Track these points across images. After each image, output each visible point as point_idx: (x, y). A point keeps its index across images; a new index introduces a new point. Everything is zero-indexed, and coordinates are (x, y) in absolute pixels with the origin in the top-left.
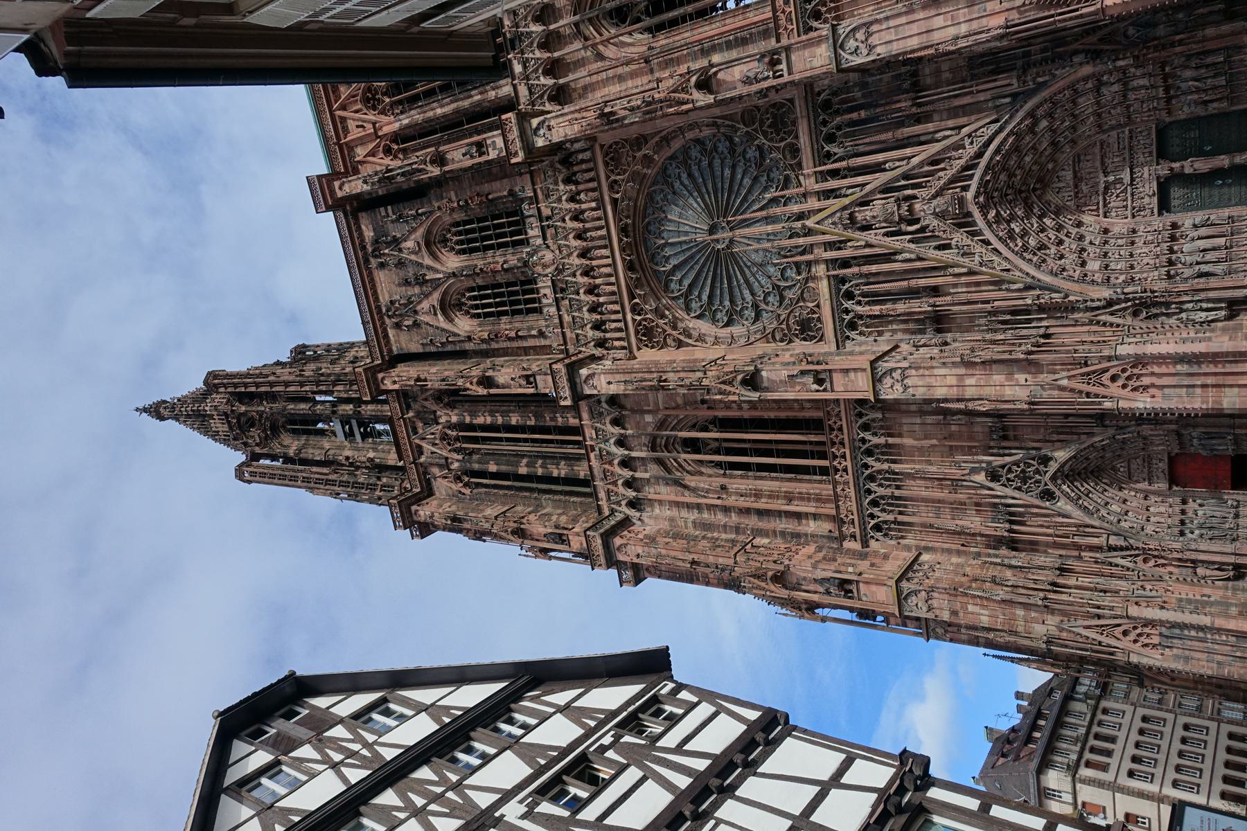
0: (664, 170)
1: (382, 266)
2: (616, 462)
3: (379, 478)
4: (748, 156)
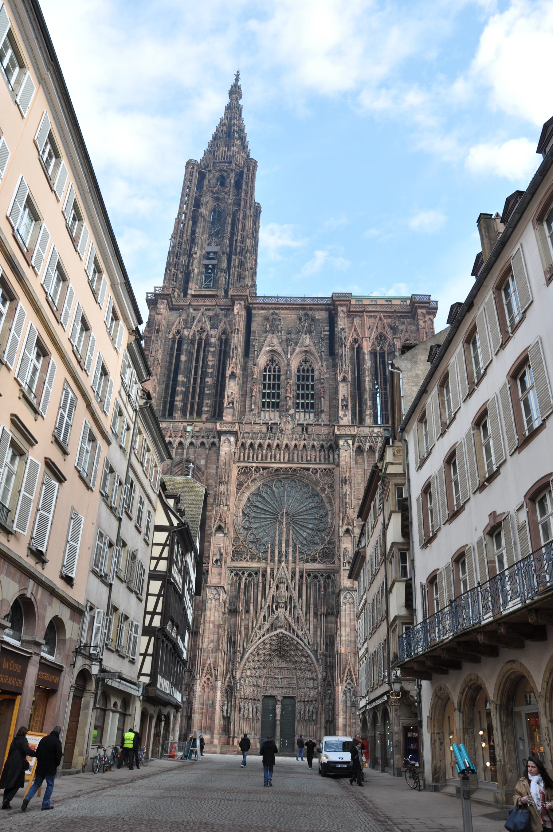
0: (318, 495)
1: (300, 319)
2: (182, 440)
3: (181, 272)
4: (316, 537)
